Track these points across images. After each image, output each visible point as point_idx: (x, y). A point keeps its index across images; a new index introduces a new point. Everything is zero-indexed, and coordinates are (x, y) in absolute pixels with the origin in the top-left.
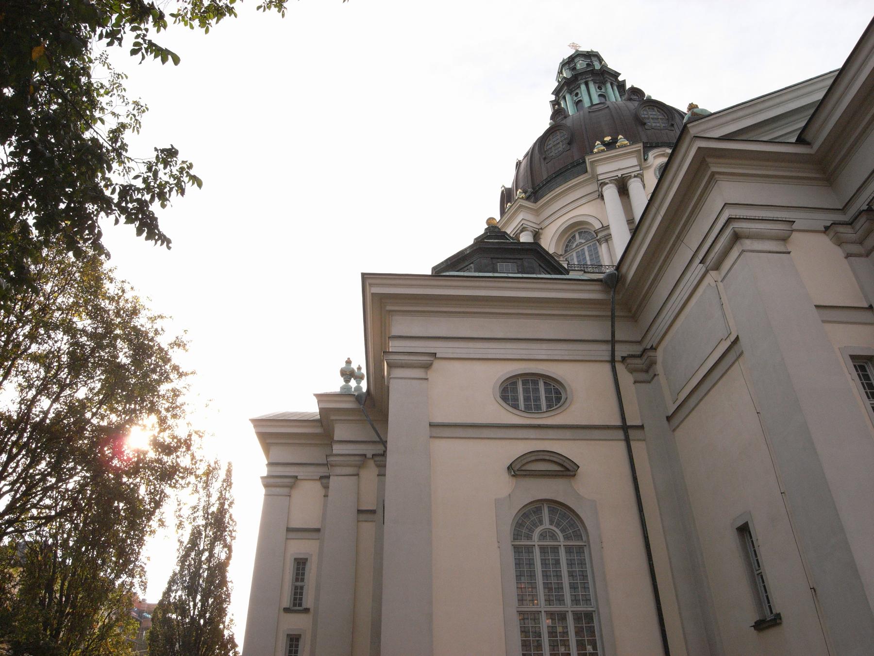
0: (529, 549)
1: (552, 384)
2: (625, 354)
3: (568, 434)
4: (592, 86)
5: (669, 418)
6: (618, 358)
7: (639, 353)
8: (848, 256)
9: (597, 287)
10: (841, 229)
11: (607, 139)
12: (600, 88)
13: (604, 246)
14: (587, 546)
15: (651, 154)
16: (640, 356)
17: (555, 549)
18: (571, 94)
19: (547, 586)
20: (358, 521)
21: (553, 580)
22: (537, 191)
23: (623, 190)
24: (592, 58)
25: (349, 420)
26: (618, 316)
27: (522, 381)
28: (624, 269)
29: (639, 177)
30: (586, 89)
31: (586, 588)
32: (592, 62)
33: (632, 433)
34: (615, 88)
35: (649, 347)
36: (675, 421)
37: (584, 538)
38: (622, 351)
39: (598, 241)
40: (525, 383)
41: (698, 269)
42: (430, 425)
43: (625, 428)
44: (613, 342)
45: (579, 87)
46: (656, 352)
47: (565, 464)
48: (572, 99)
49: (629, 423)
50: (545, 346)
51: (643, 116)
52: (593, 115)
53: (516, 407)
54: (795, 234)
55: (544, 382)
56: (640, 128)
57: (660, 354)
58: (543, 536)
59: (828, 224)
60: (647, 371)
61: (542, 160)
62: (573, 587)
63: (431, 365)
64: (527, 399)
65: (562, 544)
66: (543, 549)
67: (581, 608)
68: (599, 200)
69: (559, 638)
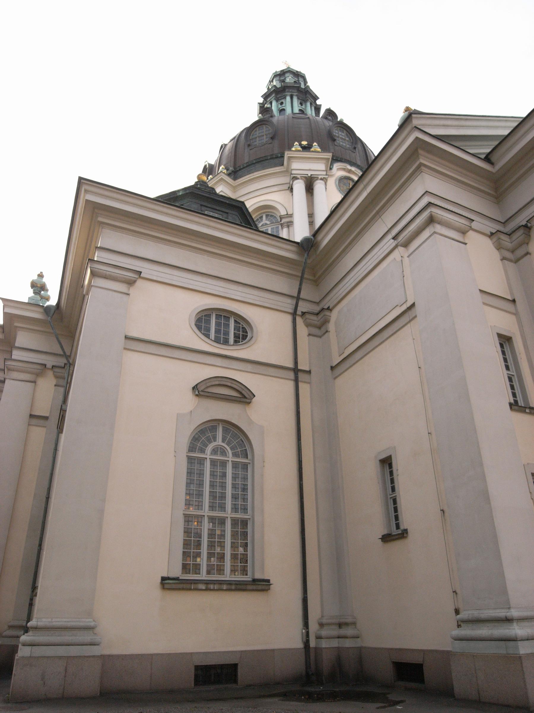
0: (201, 461)
1: (241, 323)
2: (304, 310)
3: (249, 367)
4: (295, 100)
5: (332, 368)
6: (299, 313)
7: (317, 312)
8: (503, 259)
9: (293, 248)
10: (503, 237)
11: (304, 143)
12: (301, 104)
14: (251, 464)
15: (336, 166)
16: (317, 314)
17: (224, 464)
18: (277, 101)
19: (213, 495)
20: (29, 425)
21: (218, 490)
22: (238, 171)
23: (309, 189)
24: (300, 78)
25: (34, 330)
27: (216, 315)
28: (320, 237)
29: (324, 181)
31: (245, 499)
33: (301, 376)
34: (313, 108)
35: (326, 307)
36: (337, 371)
37: (249, 456)
38: (303, 307)
39: (282, 225)
40: (218, 317)
41: (388, 243)
42: (125, 337)
43: (296, 370)
44: (298, 298)
45: (285, 98)
46: (331, 312)
47: (243, 392)
48: (278, 106)
49: (299, 368)
50: (241, 288)
51: (334, 134)
52: (295, 120)
53: (208, 336)
54: (471, 233)
55: (235, 320)
56: (330, 143)
57: (334, 315)
58: (214, 451)
59: (494, 231)
60: (320, 328)
61: (246, 146)
62: (235, 497)
63: (135, 282)
64: (217, 331)
65: (230, 459)
66: (213, 463)
67: (239, 515)
68: (288, 192)
69: (216, 540)
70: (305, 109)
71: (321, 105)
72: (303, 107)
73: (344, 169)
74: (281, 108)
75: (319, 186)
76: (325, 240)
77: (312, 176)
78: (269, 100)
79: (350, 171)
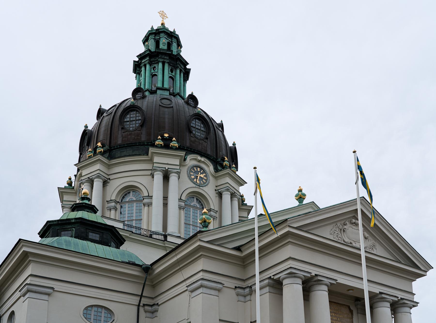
2: (145, 303)
4: (166, 66)
6: (141, 304)
11: (166, 135)
12: (172, 71)
13: (146, 208)
15: (189, 157)
18: (150, 65)
23: (166, 178)
24: (173, 39)
26: (146, 284)
29: (178, 174)
30: (162, 68)
32: (172, 42)
34: (182, 74)
35: (156, 303)
38: (144, 301)
44: (141, 296)
45: (158, 63)
48: (151, 71)
51: (192, 125)
52: (162, 109)
56: (187, 134)
57: (161, 308)
61: (120, 129)
68: (150, 177)
70: (175, 76)
71: (191, 69)
72: (173, 74)
73: (195, 159)
74: (154, 73)
75: (173, 178)
76: (159, 269)
77: (169, 170)
78: (144, 62)
79: (199, 161)
